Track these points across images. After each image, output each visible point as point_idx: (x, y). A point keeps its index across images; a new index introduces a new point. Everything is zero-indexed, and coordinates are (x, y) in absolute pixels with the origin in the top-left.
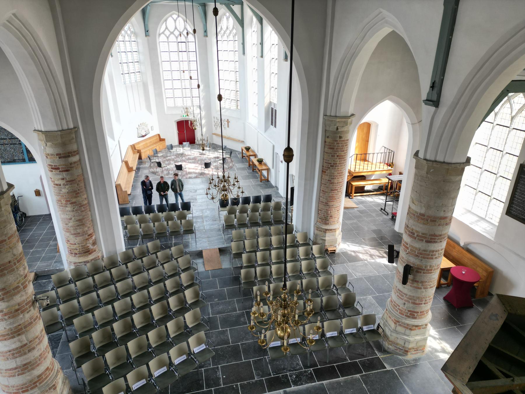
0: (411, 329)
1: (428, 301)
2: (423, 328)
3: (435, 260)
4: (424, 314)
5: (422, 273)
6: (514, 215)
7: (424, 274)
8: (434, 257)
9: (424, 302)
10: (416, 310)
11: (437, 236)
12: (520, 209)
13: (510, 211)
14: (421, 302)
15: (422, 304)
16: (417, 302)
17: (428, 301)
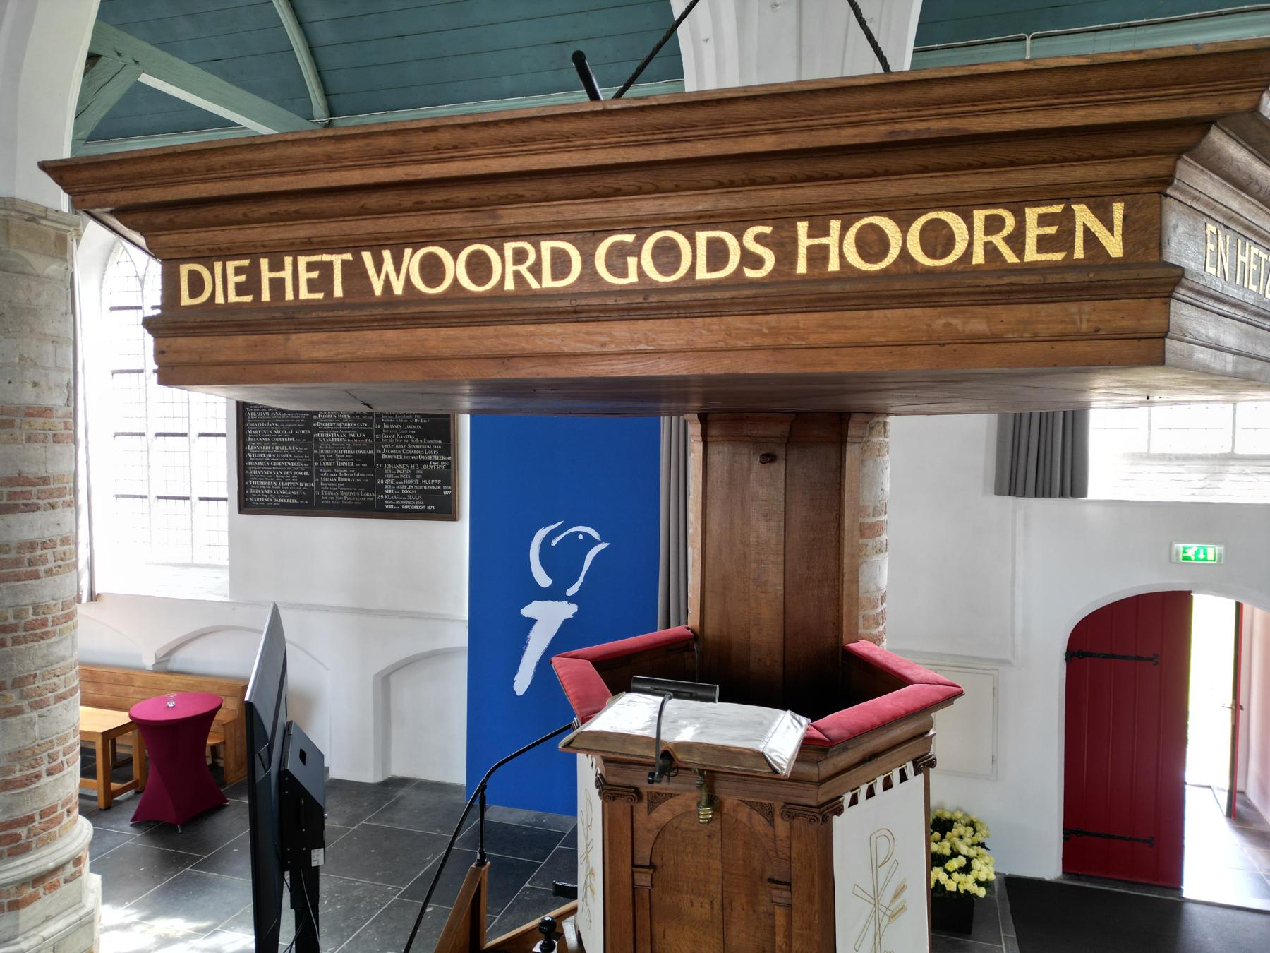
0: (15, 906)
1: (64, 759)
2: (66, 881)
3: (46, 580)
4: (58, 820)
5: (9, 642)
6: (259, 506)
7: (19, 643)
8: (42, 568)
9: (44, 767)
10: (18, 814)
11: (33, 484)
12: (269, 483)
13: (247, 499)
14: (32, 771)
15: (38, 776)
16: (18, 774)
17: (61, 758)
